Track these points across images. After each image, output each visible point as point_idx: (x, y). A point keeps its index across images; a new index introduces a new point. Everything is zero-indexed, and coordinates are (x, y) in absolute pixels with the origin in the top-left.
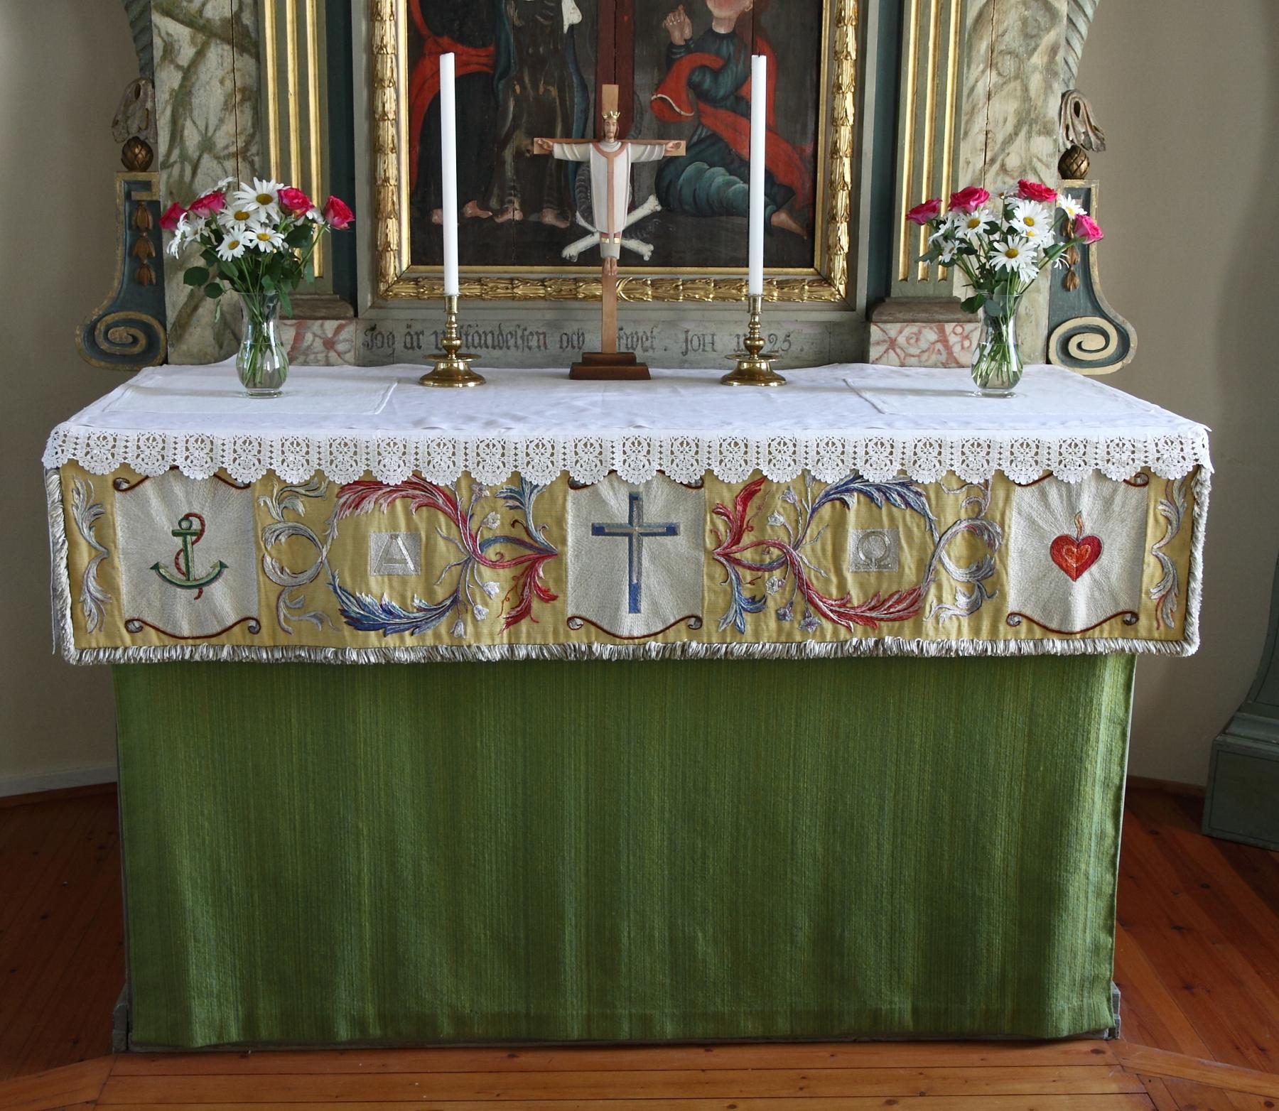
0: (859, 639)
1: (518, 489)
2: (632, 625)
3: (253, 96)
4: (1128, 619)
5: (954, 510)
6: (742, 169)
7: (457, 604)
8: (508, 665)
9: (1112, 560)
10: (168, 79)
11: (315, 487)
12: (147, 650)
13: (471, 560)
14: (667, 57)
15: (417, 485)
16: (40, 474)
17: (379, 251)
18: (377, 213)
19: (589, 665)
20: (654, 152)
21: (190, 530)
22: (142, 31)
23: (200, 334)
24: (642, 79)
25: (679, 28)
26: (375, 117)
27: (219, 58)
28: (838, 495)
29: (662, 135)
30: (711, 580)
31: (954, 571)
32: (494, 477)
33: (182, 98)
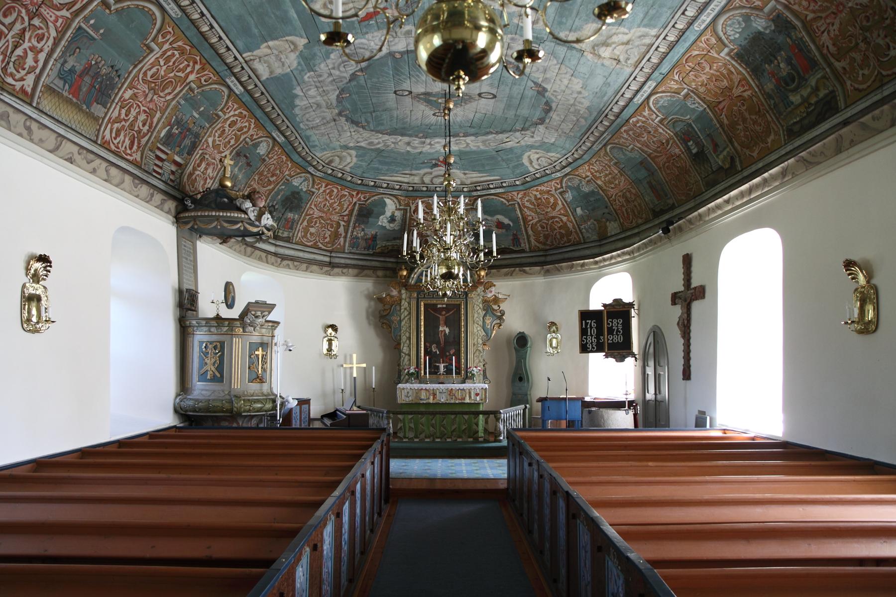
0: (460, 401)
1: (433, 389)
2: (442, 400)
3: (410, 360)
4: (482, 400)
5: (467, 391)
6: (453, 365)
7: (429, 398)
8: (433, 403)
9: (480, 395)
10: (402, 359)
11: (418, 389)
12: (404, 402)
13: (430, 395)
14: (447, 356)
15: (426, 389)
16: (397, 388)
17: (421, 374)
18: (421, 370)
19: (439, 403)
20: (445, 364)
21: (408, 393)
22: (400, 355)
23: (404, 381)
24: (445, 358)
25: (448, 354)
26: (421, 362)
27: (407, 357)
28: (458, 390)
29: (446, 363)
30: (449, 397)
31: (468, 396)
32: (432, 388)
33: (403, 360)
